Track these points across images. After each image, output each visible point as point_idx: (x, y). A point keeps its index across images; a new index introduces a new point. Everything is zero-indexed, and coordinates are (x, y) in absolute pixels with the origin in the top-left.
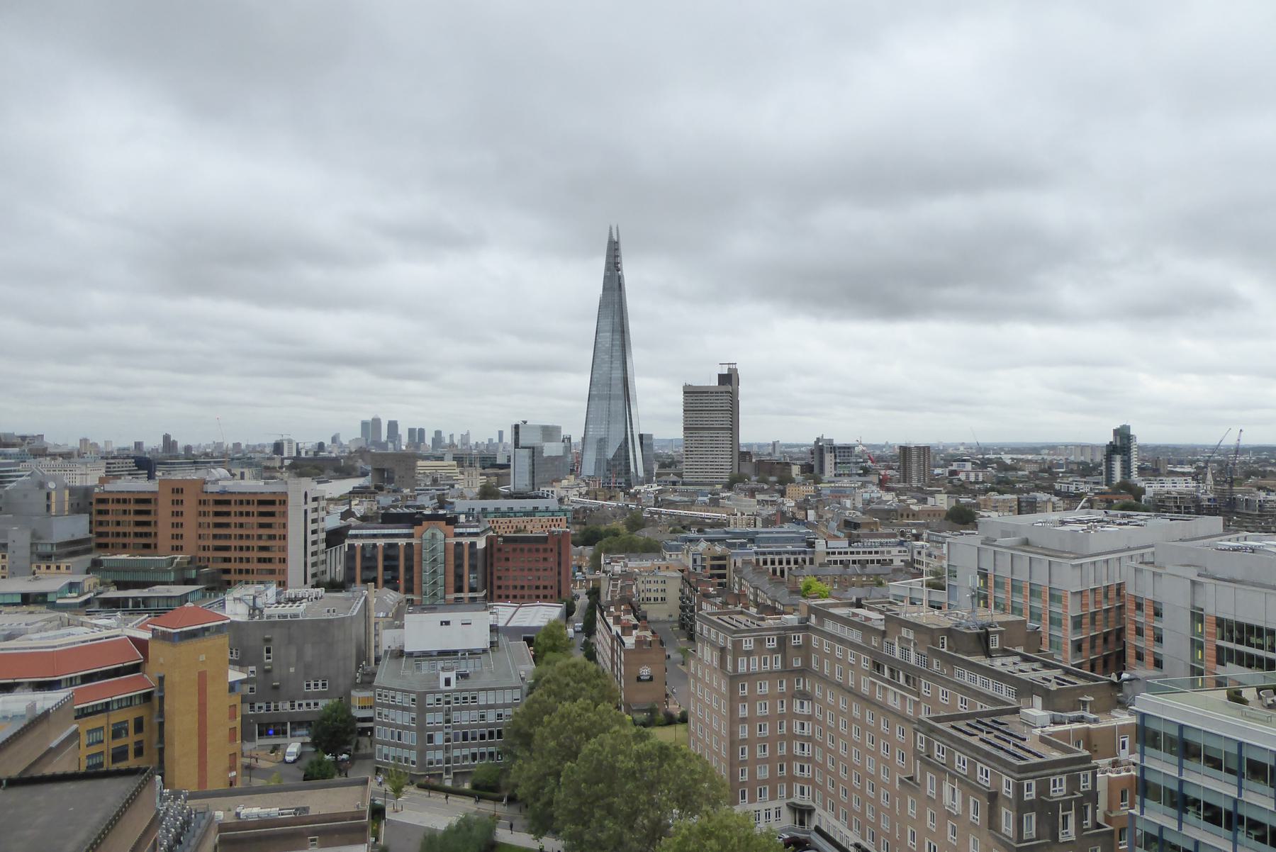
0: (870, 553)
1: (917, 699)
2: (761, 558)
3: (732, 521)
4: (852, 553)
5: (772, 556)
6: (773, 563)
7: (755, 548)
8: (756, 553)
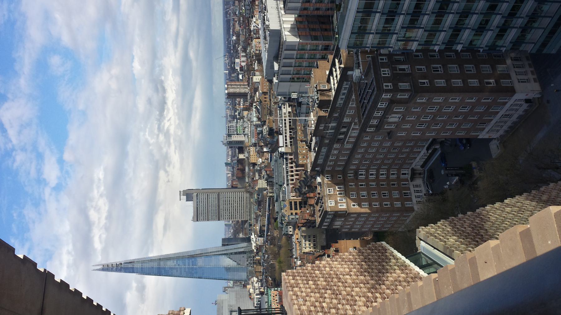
0: (285, 124)
1: (353, 124)
2: (290, 182)
3: (271, 195)
4: (286, 133)
5: (289, 177)
6: (292, 176)
7: (285, 185)
8: (288, 185)
